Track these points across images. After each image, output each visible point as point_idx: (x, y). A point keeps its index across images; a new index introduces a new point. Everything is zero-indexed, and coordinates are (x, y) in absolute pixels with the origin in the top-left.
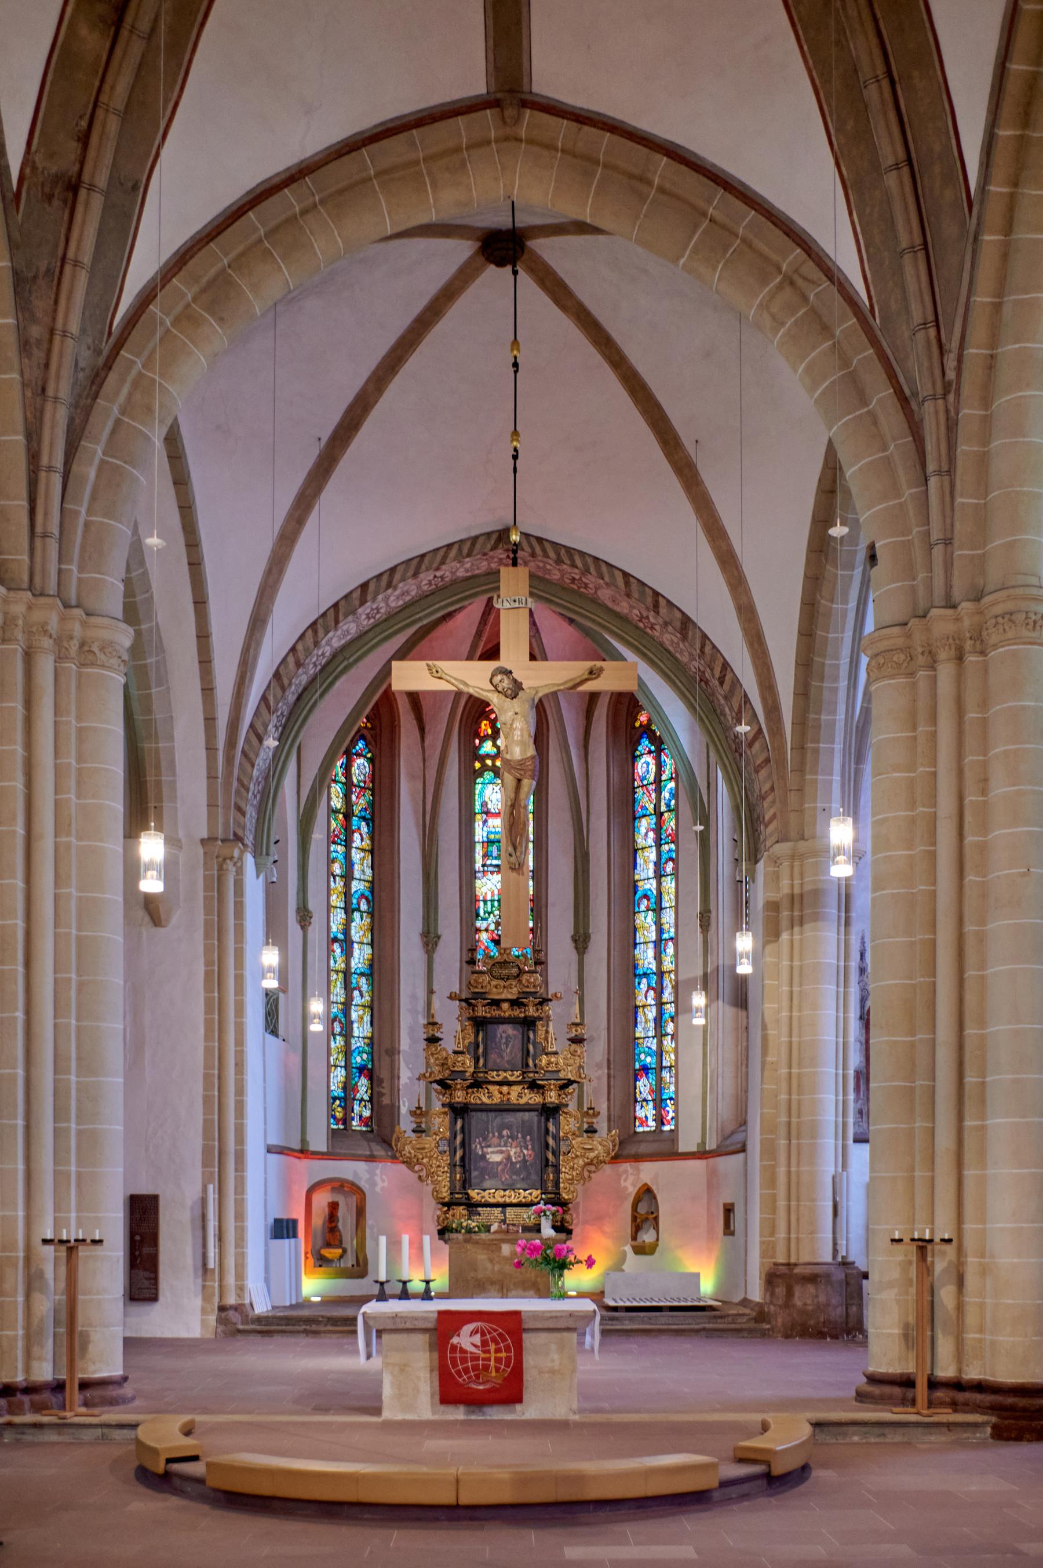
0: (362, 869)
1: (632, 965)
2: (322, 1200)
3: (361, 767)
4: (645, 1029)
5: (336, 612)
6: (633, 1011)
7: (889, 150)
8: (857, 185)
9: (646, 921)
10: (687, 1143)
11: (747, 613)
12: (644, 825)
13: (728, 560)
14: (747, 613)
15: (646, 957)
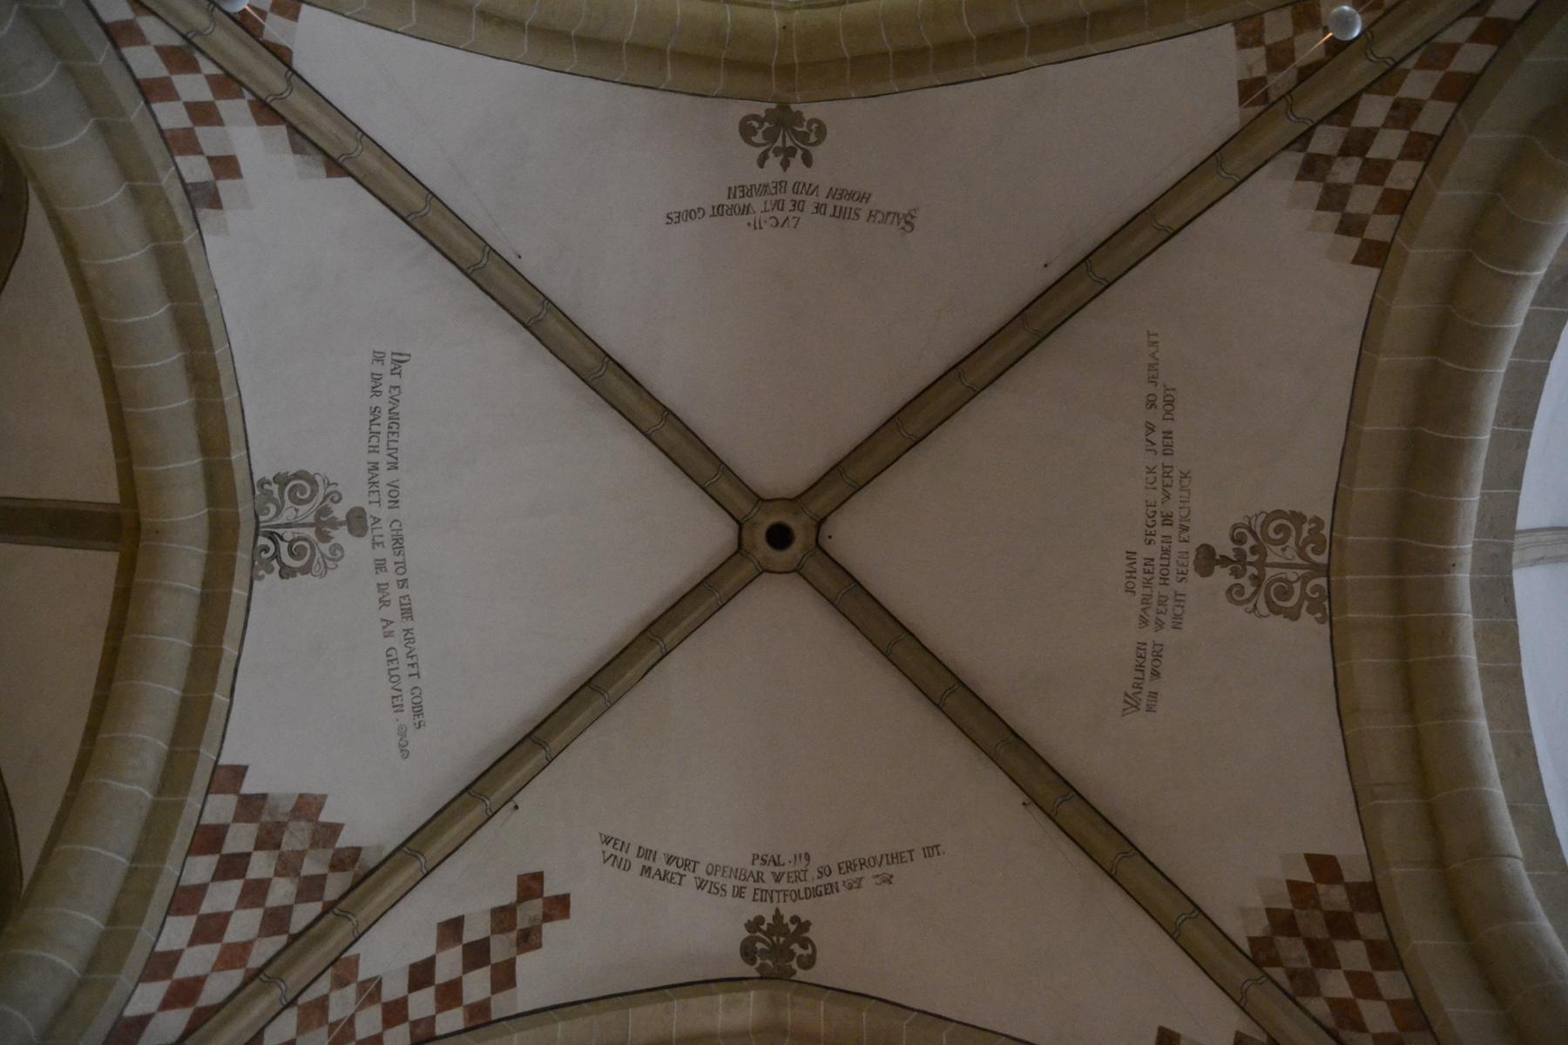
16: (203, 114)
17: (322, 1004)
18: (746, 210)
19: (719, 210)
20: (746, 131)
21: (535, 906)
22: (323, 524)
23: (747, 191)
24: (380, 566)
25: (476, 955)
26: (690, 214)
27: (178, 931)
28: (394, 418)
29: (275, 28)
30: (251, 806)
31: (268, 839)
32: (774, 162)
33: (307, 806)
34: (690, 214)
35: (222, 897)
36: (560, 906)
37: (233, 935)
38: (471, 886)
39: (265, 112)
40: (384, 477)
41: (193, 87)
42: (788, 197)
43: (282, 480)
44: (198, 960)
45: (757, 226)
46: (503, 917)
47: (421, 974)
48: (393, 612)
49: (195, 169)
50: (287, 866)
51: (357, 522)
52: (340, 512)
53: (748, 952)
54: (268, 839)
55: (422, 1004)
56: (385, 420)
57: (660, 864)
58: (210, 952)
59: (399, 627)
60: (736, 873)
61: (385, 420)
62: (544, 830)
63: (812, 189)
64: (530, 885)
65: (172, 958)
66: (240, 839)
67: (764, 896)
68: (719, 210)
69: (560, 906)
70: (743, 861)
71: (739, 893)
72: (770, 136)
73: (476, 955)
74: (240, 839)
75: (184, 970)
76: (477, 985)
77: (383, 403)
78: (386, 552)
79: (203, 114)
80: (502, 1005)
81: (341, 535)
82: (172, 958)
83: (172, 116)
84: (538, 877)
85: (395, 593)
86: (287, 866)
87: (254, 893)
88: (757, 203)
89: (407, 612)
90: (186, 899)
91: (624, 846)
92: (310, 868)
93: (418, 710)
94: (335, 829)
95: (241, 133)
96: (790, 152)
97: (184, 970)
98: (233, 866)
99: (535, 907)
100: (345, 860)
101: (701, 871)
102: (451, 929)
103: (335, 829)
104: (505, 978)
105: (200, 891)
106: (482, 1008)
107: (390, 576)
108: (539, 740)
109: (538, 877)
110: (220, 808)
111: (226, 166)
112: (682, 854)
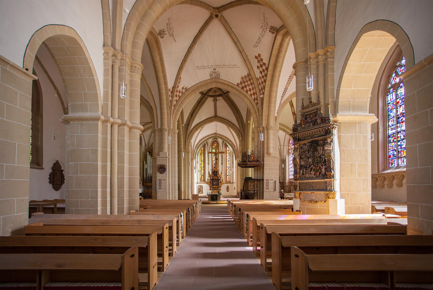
0: (203, 158)
1: (226, 167)
2: (199, 187)
3: (202, 149)
4: (228, 172)
5: (201, 140)
6: (227, 170)
7: (240, 122)
8: (238, 123)
9: (228, 162)
10: (231, 182)
11: (235, 140)
12: (228, 154)
13: (233, 136)
14: (235, 140)
15: (228, 165)
16: (180, 92)
17: (260, 83)
18: (172, 33)
19: (173, 36)
20: (163, 37)
21: (258, 57)
22: (215, 73)
23: (170, 34)
24: (219, 68)
25: (261, 66)
26: (174, 40)
27: (249, 93)
28: (203, 66)
29: (171, 90)
30: (241, 83)
31: (244, 82)
32: (165, 33)
33: (242, 78)
34: (174, 40)
35: (248, 88)
36: (259, 55)
37: (251, 88)
38: (255, 64)
39: (178, 87)
40: (210, 67)
41: (178, 94)
42: (169, 29)
43: (210, 76)
44: (252, 92)
45: (174, 31)
46: (259, 62)
47: (261, 72)
48: (224, 67)
49: (184, 91)
50: (247, 82)
51: (215, 69)
52: (214, 71)
53: (273, 33)
54: (244, 82)
55: (263, 74)
56: (204, 67)
57: (258, 41)
58: (252, 90)
59: (226, 66)
60: (262, 32)
61: (204, 67)
62: (252, 53)
63: (167, 28)
64: (256, 57)
65: (251, 94)
66: (243, 85)
67: (266, 29)
68: (173, 36)
69: (259, 55)
70: (261, 30)
71: (265, 32)
72: (162, 34)
73: (261, 66)
74: (243, 85)
75: (252, 93)
76: (264, 67)
77: (202, 68)
78: (218, 67)
79: (180, 92)
80: (267, 66)
81: (216, 71)
82: (251, 94)
83: (181, 94)
84: (256, 56)
85: (222, 66)
86: (247, 82)
87: (248, 85)
88: (171, 33)
89: (224, 65)
90: (247, 91)
91: (255, 45)
92: (248, 79)
93: (235, 65)
94: (245, 76)
95: (180, 88)
96: (163, 32)
97: (252, 93)
98: (246, 86)
99: (259, 58)
100: (249, 75)
101: (261, 36)
102: (258, 67)
103: (245, 76)
104: (264, 64)
105: (247, 90)
106: (266, 68)
107: (220, 67)
108: (241, 52)
109: (256, 56)
110: (240, 86)
111: (183, 88)
112: (258, 38)
